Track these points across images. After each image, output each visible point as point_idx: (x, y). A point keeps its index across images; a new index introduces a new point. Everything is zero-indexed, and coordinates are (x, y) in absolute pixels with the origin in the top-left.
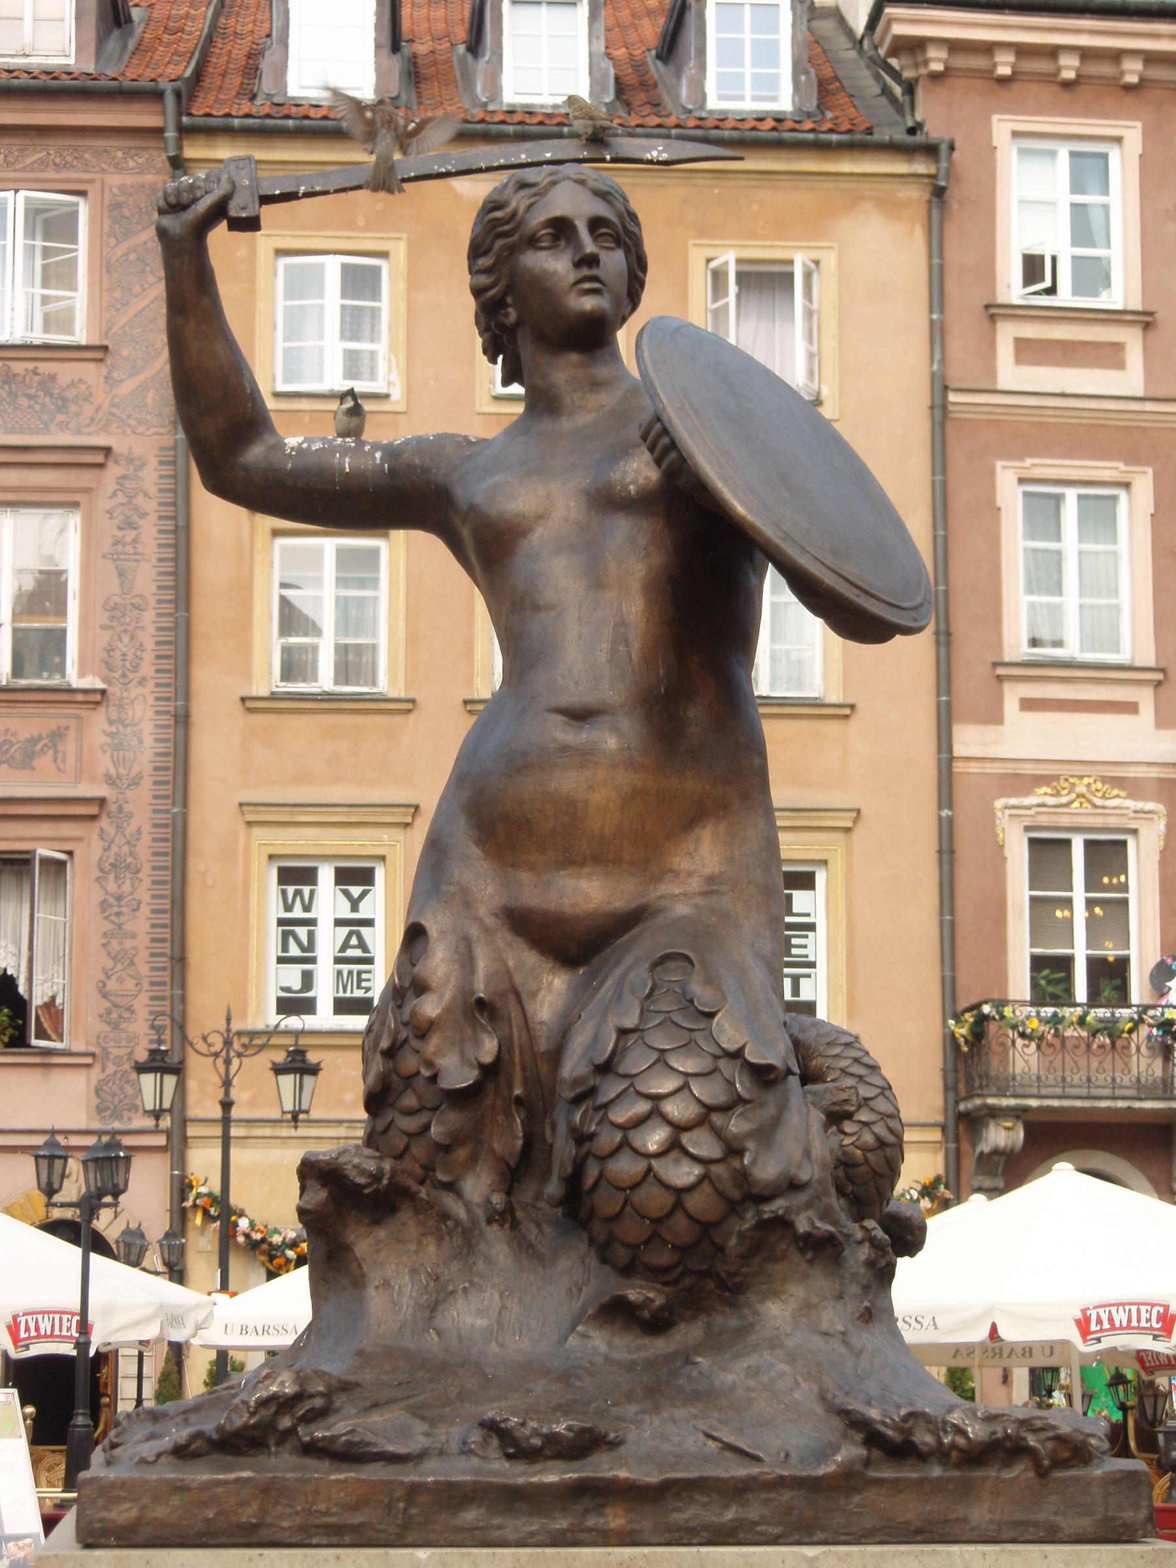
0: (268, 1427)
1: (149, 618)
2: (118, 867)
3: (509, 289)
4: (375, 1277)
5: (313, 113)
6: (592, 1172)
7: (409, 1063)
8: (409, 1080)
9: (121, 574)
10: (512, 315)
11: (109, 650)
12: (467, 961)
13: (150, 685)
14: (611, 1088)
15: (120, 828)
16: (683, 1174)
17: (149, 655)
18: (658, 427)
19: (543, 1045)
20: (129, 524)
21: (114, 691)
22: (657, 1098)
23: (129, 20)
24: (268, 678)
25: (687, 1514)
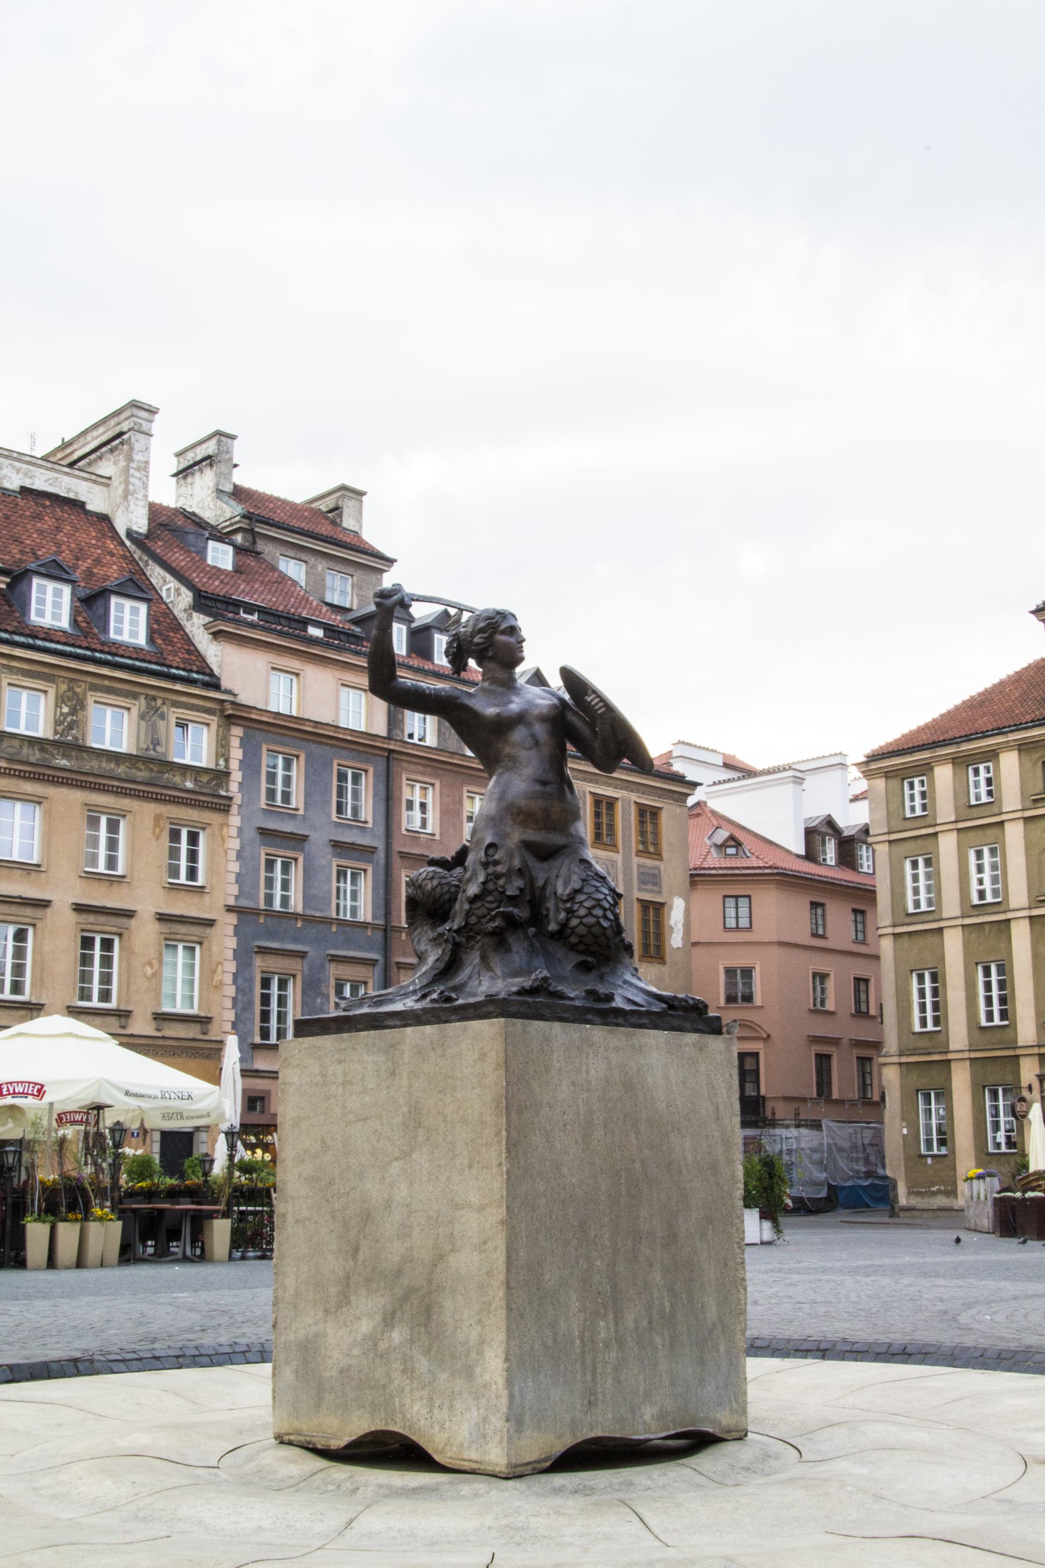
0: (542, 986)
3: (490, 645)
4: (514, 950)
6: (574, 922)
7: (491, 886)
8: (490, 893)
10: (491, 654)
12: (511, 856)
14: (580, 898)
16: (605, 924)
18: (597, 700)
19: (540, 883)
22: (599, 900)
25: (633, 1020)
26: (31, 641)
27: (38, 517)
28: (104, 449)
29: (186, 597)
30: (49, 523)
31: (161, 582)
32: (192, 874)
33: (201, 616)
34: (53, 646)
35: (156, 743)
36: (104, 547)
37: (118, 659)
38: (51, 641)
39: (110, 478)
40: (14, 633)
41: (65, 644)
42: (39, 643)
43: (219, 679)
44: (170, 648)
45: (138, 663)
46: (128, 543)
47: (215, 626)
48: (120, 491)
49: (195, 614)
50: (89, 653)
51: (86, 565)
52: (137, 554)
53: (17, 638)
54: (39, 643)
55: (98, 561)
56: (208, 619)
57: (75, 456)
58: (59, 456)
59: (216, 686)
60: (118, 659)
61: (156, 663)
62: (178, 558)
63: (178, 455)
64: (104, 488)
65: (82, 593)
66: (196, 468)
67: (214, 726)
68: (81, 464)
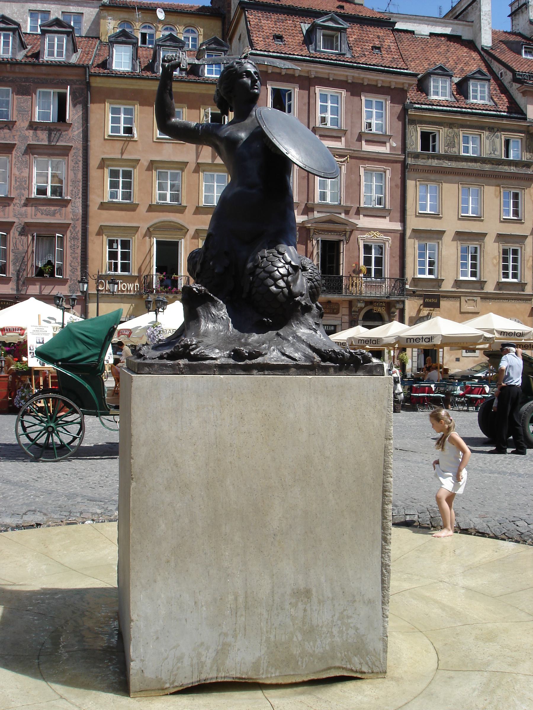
1: (81, 184)
2: (74, 238)
5: (118, 73)
9: (75, 174)
11: (72, 191)
13: (81, 199)
15: (74, 230)
17: (81, 192)
20: (77, 163)
21: (73, 200)
23: (77, 51)
24: (107, 198)
26: (430, 107)
27: (437, 46)
28: (470, 8)
29: (510, 75)
30: (443, 48)
31: (498, 70)
32: (516, 213)
33: (517, 84)
34: (441, 108)
35: (494, 150)
36: (470, 57)
37: (474, 111)
38: (440, 106)
39: (473, 22)
40: (422, 104)
41: (447, 106)
42: (435, 107)
43: (526, 115)
44: (501, 102)
45: (484, 112)
46: (482, 53)
47: (523, 89)
48: (478, 26)
49: (514, 84)
50: (459, 109)
51: (460, 66)
52: (487, 57)
53: (423, 106)
54: (435, 107)
55: (467, 64)
56: (520, 85)
57: (457, 14)
58: (451, 15)
59: (525, 119)
60: (474, 111)
61: (494, 111)
62: (508, 57)
63: (511, 5)
64: (471, 28)
65: (456, 80)
66: (520, 10)
67: (524, 140)
68: (460, 17)
